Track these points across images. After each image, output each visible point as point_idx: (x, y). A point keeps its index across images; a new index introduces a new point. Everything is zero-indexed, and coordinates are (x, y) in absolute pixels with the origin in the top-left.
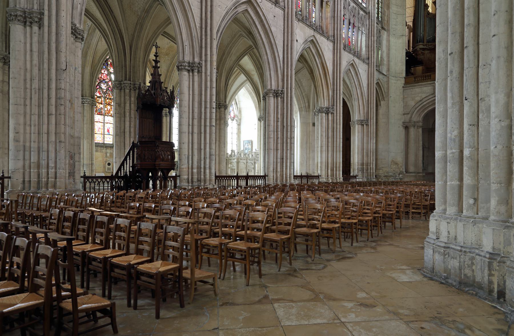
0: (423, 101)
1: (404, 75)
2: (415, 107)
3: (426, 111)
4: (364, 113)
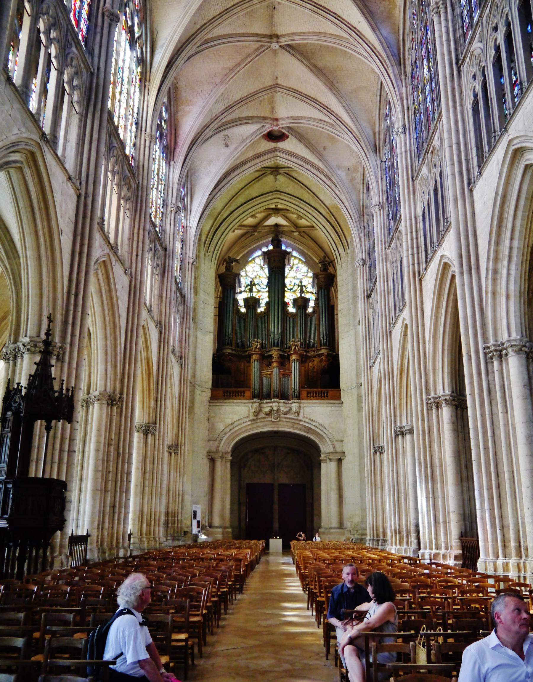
0: (234, 425)
1: (210, 385)
2: (223, 433)
3: (237, 440)
4: (172, 436)
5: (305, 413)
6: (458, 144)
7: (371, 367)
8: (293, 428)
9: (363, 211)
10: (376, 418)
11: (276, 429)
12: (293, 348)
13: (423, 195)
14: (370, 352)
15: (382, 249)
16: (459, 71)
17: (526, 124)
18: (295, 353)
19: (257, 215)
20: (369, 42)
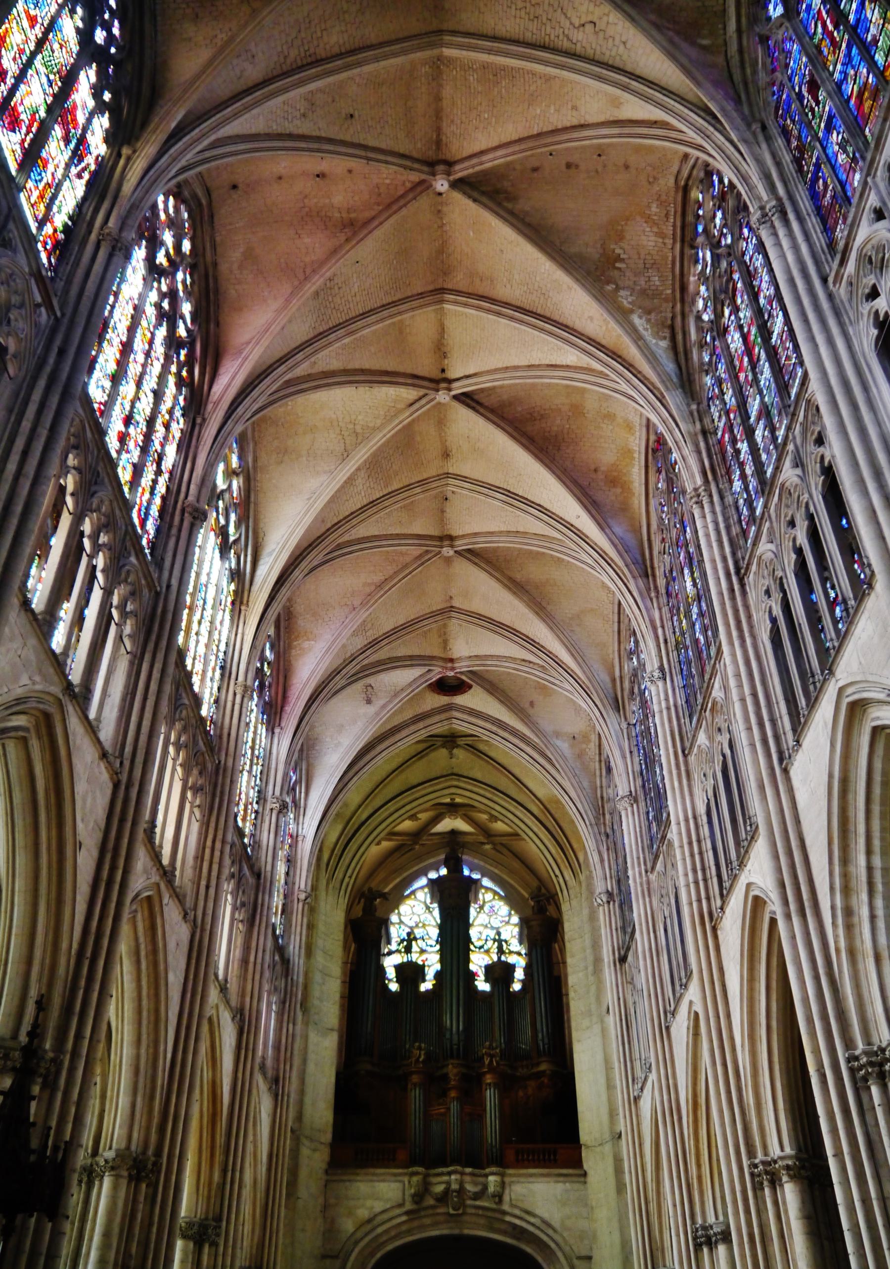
0: (375, 1222)
1: (328, 1137)
3: (379, 1255)
5: (513, 1197)
6: (755, 695)
7: (637, 1099)
8: (492, 1229)
9: (603, 807)
10: (653, 1207)
11: (456, 1232)
12: (487, 1062)
13: (704, 779)
14: (632, 1068)
15: (640, 874)
16: (742, 585)
17: (863, 662)
18: (491, 1070)
19: (419, 816)
20: (596, 544)
